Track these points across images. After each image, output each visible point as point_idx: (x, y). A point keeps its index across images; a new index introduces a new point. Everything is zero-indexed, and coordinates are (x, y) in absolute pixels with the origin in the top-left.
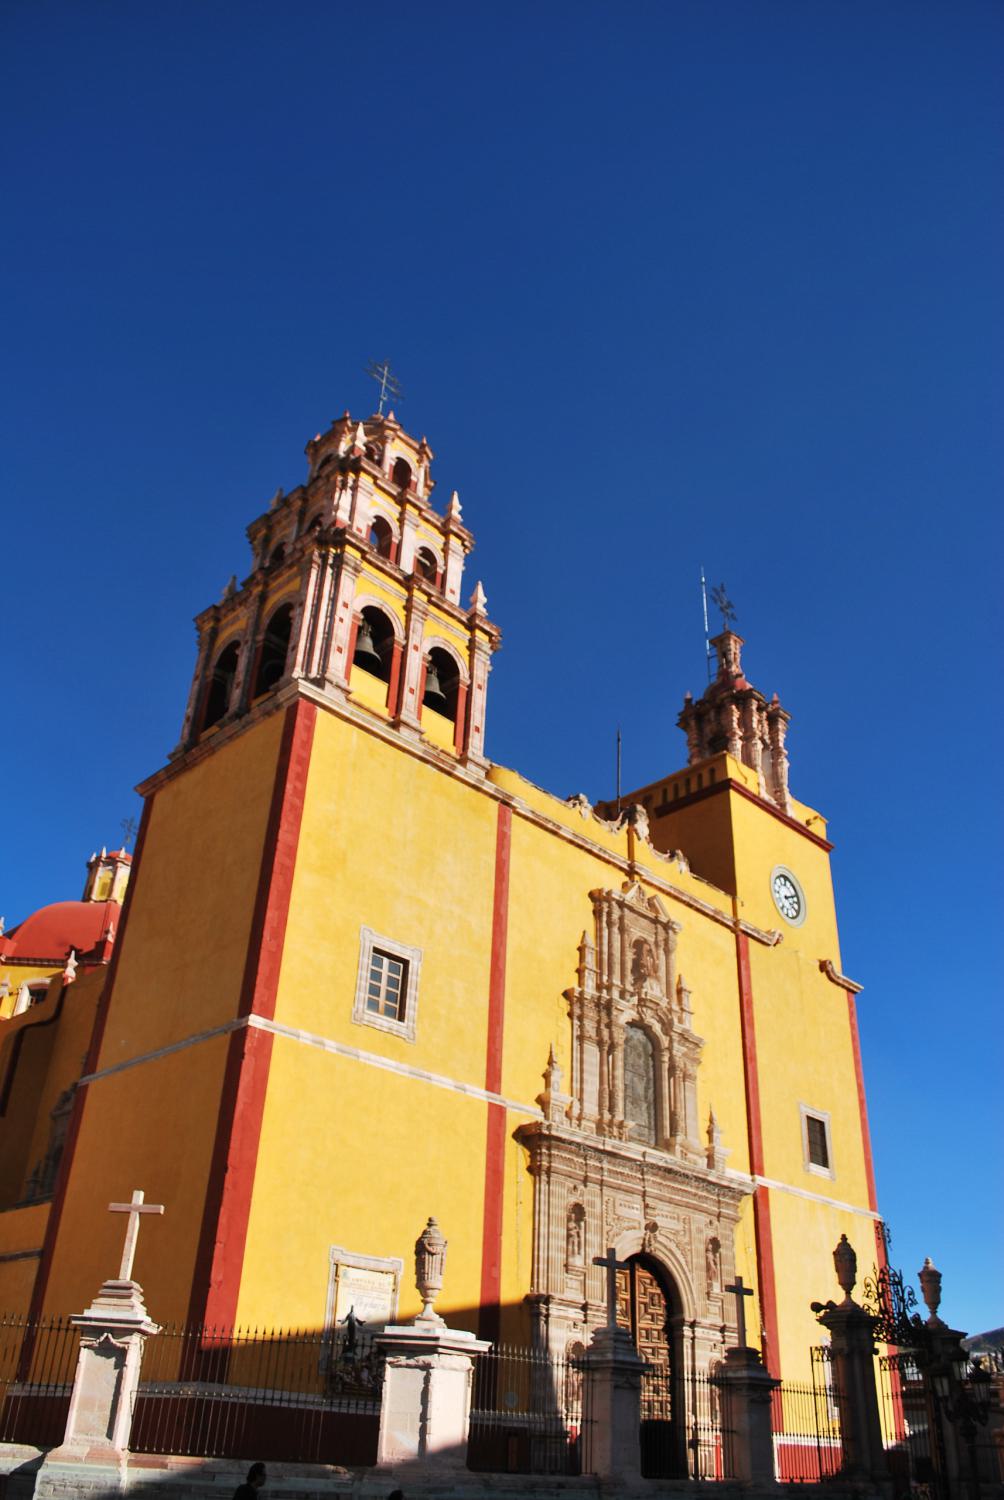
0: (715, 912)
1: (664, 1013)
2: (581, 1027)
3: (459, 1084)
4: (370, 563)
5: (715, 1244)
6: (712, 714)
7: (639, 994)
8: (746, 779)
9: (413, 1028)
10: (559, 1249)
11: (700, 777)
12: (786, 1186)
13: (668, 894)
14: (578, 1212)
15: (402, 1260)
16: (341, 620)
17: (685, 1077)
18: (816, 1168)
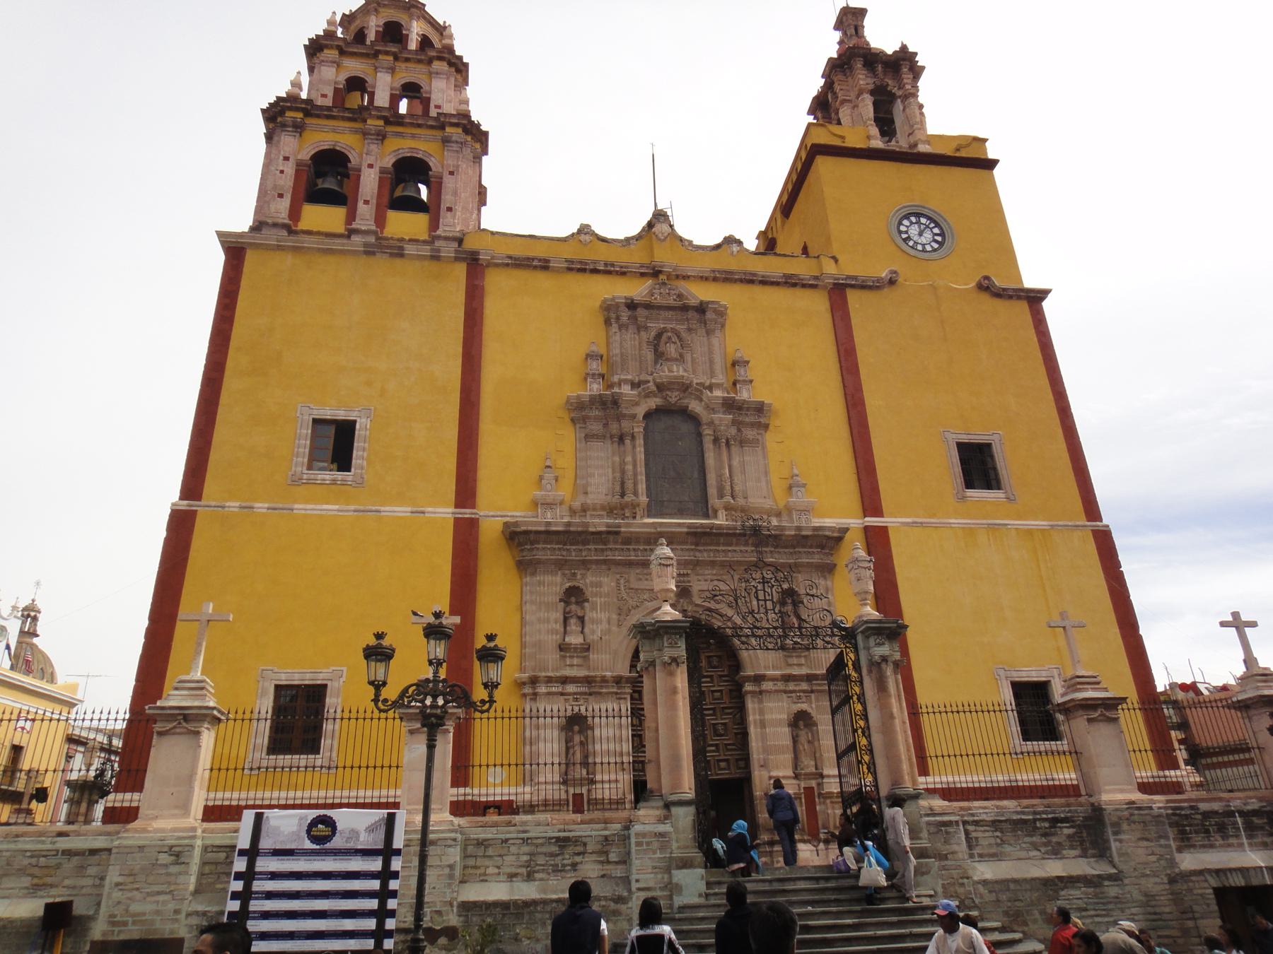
0: (785, 276)
1: (697, 390)
3: (415, 509)
8: (843, 137)
9: (361, 474)
10: (554, 632)
13: (715, 279)
14: (574, 595)
15: (345, 669)
16: (282, 172)
18: (970, 492)
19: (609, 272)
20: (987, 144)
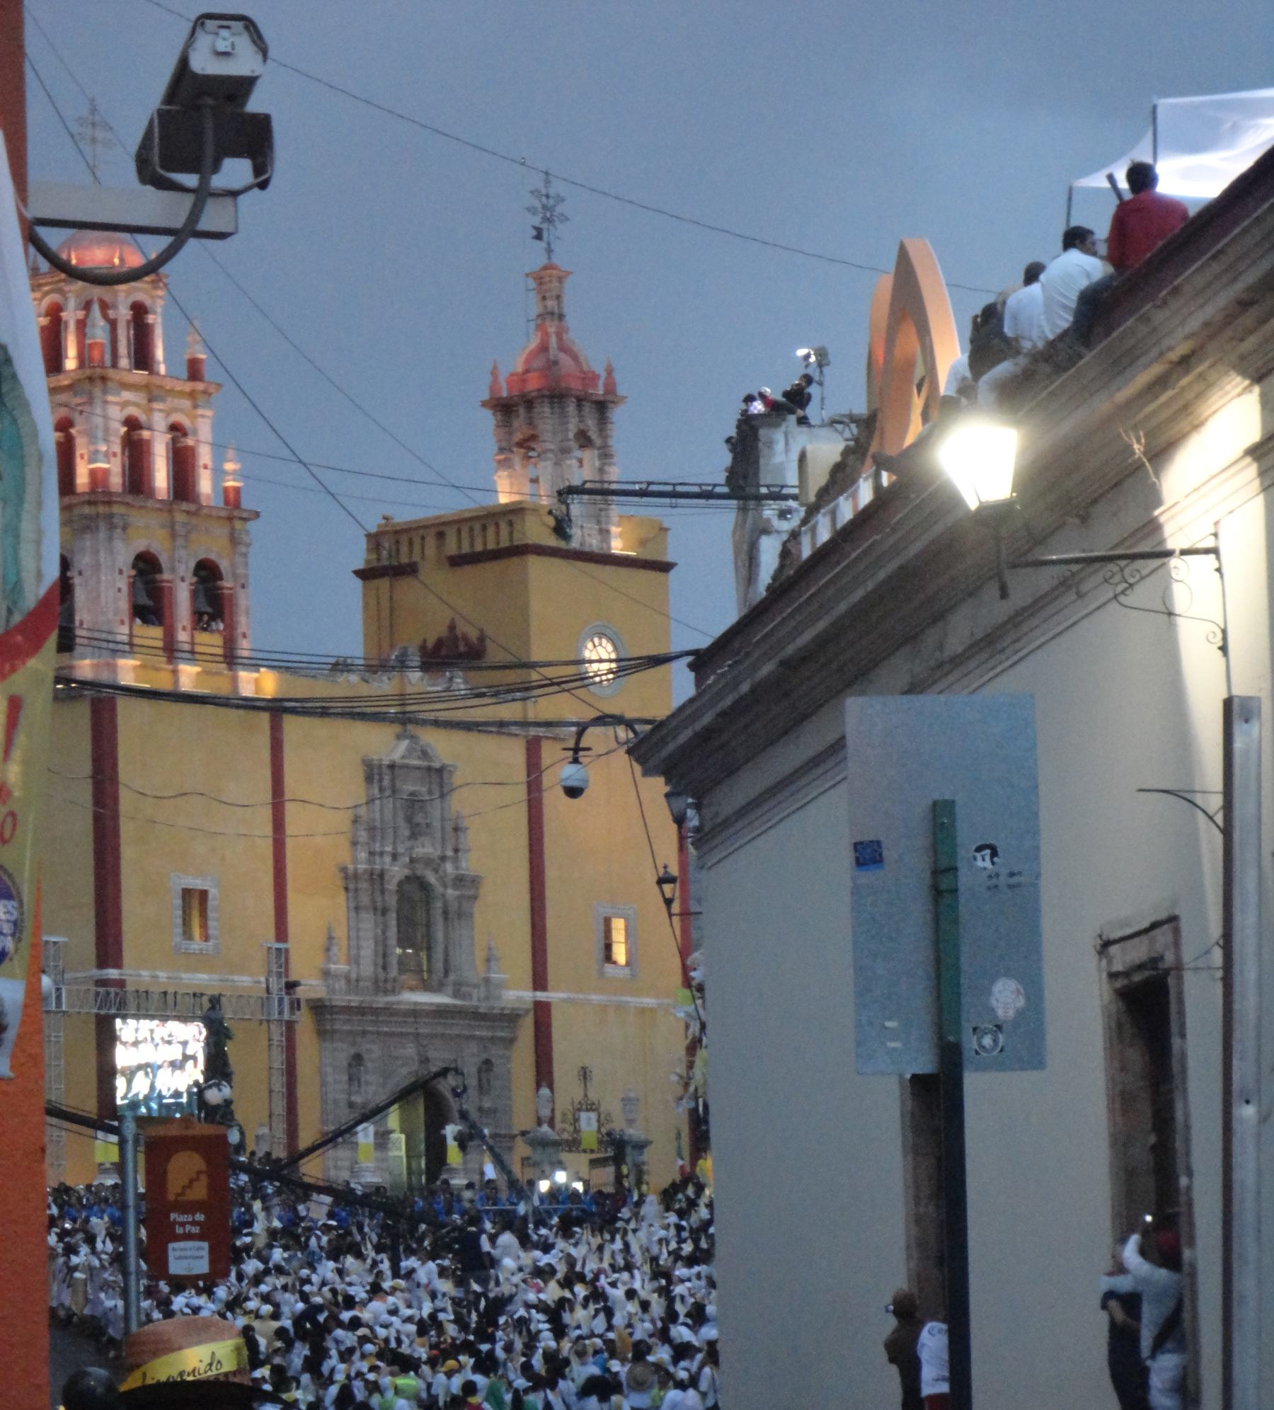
2: (356, 898)
4: (133, 506)
6: (522, 411)
7: (410, 854)
11: (497, 525)
12: (572, 995)
14: (358, 1059)
16: (119, 590)
17: (460, 915)
20: (670, 533)
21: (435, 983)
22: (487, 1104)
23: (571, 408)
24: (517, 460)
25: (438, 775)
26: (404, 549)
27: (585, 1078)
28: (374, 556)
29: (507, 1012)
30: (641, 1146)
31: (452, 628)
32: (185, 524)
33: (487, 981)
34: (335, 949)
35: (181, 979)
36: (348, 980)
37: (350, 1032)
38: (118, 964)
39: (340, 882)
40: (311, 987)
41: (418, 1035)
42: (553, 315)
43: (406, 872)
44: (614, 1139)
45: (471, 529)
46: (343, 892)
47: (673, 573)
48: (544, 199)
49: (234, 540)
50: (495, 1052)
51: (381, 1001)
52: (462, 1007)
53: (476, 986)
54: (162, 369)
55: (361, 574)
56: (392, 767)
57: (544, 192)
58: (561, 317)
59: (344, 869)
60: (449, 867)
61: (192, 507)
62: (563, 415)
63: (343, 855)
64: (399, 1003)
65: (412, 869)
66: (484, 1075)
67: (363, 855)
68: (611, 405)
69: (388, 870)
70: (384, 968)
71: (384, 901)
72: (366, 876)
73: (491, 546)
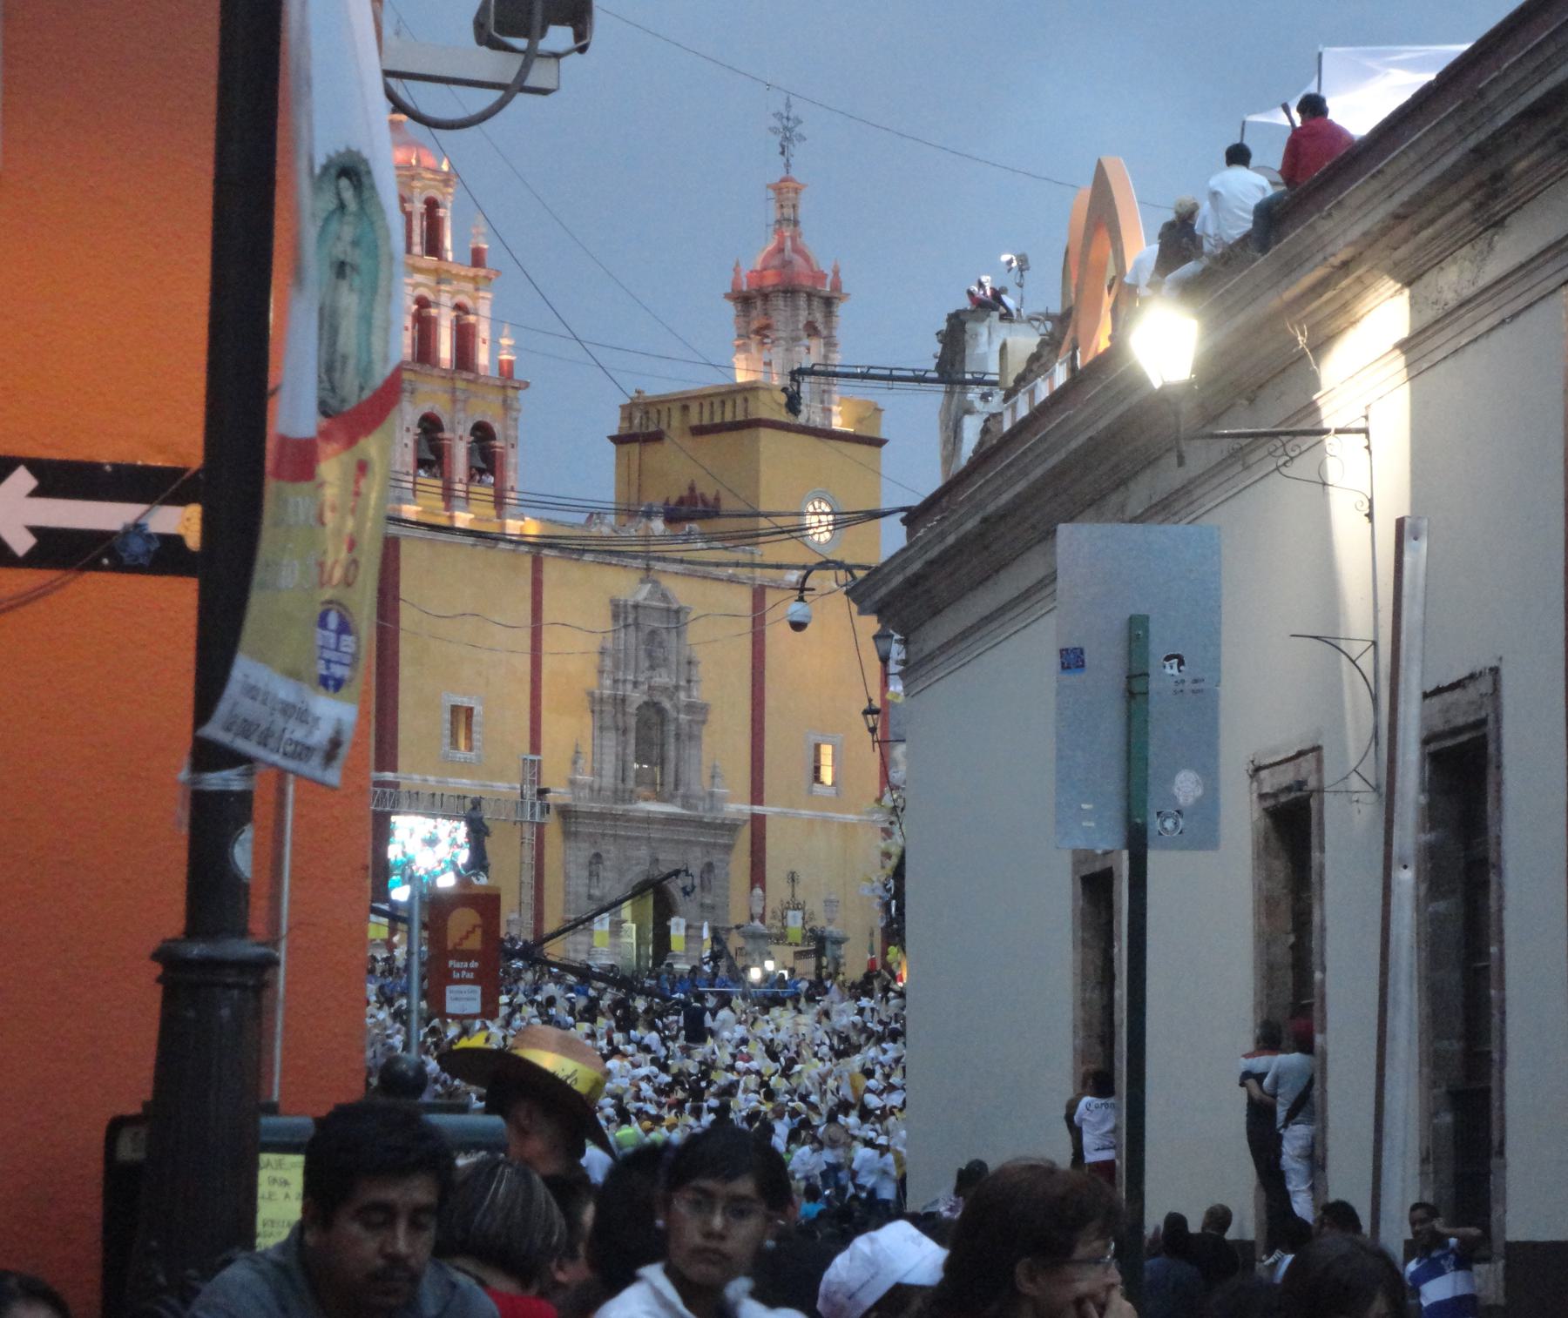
2: (602, 719)
4: (420, 373)
5: (709, 867)
6: (759, 303)
12: (785, 810)
14: (598, 857)
16: (406, 445)
17: (691, 737)
19: (616, 565)
20: (883, 413)
21: (666, 795)
22: (708, 901)
23: (802, 301)
24: (754, 347)
25: (676, 616)
26: (653, 415)
27: (793, 880)
28: (626, 425)
29: (727, 822)
30: (838, 942)
31: (692, 489)
32: (464, 391)
33: (712, 795)
34: (581, 762)
35: (448, 783)
36: (591, 789)
37: (591, 835)
38: (394, 769)
39: (586, 704)
40: (559, 794)
41: (650, 838)
42: (788, 222)
43: (645, 698)
44: (817, 935)
45: (712, 404)
46: (590, 714)
47: (885, 447)
48: (785, 121)
49: (506, 405)
50: (716, 857)
51: (620, 808)
52: (690, 816)
53: (702, 799)
54: (450, 256)
55: (614, 439)
56: (636, 607)
57: (785, 115)
58: (796, 223)
59: (591, 694)
60: (682, 695)
61: (471, 376)
62: (796, 308)
63: (591, 681)
64: (636, 811)
65: (650, 696)
66: (705, 876)
67: (608, 682)
68: (835, 301)
69: (629, 696)
70: (623, 780)
71: (625, 722)
72: (610, 700)
73: (728, 417)
